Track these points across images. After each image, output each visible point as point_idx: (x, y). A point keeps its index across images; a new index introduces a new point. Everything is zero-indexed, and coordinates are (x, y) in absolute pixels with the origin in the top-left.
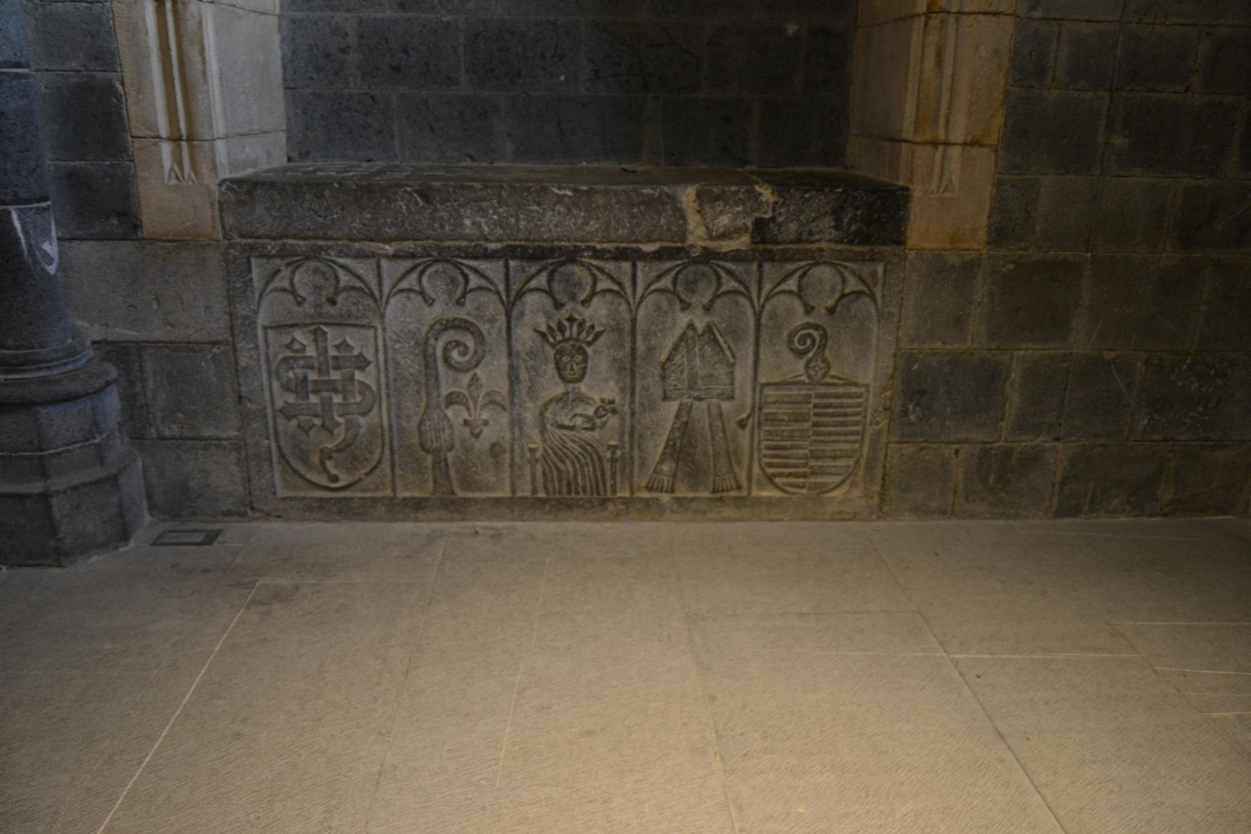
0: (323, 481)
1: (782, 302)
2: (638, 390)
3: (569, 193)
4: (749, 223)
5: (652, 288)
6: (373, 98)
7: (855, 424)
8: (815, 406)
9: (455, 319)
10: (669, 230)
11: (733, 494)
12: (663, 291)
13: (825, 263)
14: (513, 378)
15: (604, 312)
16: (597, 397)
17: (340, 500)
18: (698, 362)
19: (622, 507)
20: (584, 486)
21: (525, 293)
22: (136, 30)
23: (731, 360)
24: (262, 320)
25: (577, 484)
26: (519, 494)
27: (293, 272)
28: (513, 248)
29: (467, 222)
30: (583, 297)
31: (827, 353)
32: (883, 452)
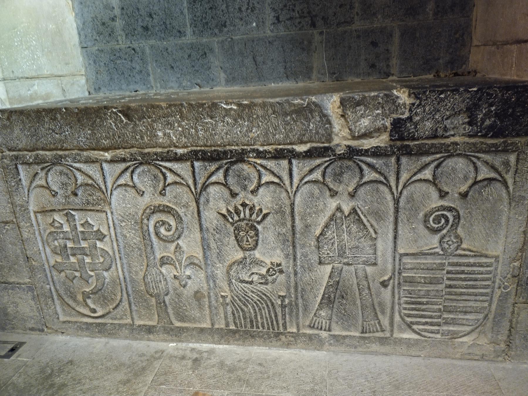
0: (86, 312)
1: (419, 189)
2: (299, 257)
3: (235, 107)
4: (388, 124)
5: (306, 180)
6: (134, 49)
7: (485, 287)
8: (448, 272)
9: (160, 205)
10: (317, 133)
11: (380, 334)
12: (315, 182)
13: (459, 155)
14: (205, 247)
15: (268, 199)
16: (268, 261)
17: (99, 325)
18: (345, 236)
19: (292, 339)
20: (263, 324)
21: (208, 186)
23: (374, 236)
24: (32, 208)
25: (257, 321)
26: (216, 326)
27: (47, 174)
28: (196, 152)
29: (160, 134)
30: (252, 188)
31: (460, 231)
32: (511, 309)
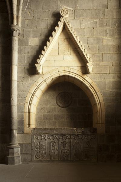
0: (39, 158)
1: (85, 139)
16: (67, 149)
22: (26, 115)
